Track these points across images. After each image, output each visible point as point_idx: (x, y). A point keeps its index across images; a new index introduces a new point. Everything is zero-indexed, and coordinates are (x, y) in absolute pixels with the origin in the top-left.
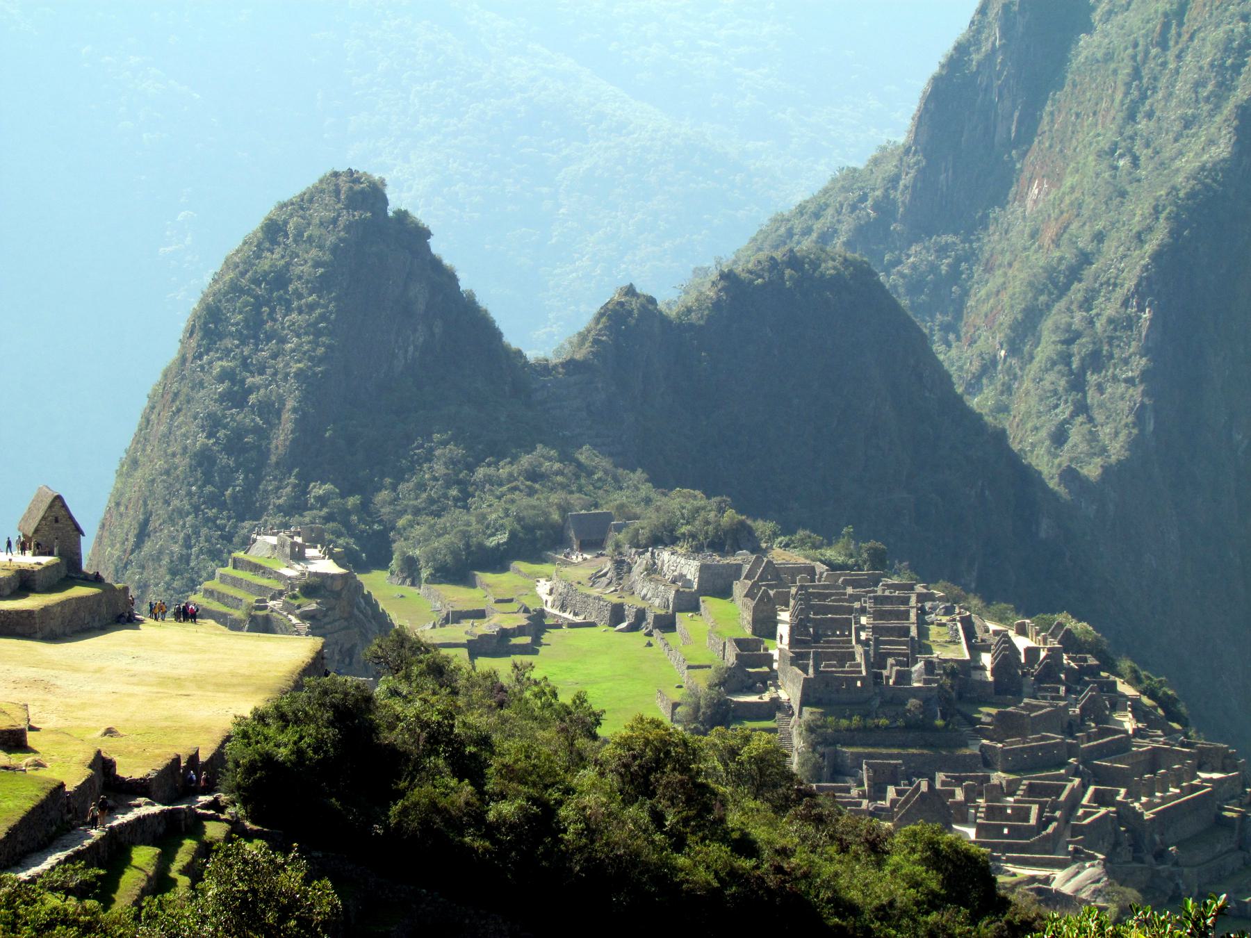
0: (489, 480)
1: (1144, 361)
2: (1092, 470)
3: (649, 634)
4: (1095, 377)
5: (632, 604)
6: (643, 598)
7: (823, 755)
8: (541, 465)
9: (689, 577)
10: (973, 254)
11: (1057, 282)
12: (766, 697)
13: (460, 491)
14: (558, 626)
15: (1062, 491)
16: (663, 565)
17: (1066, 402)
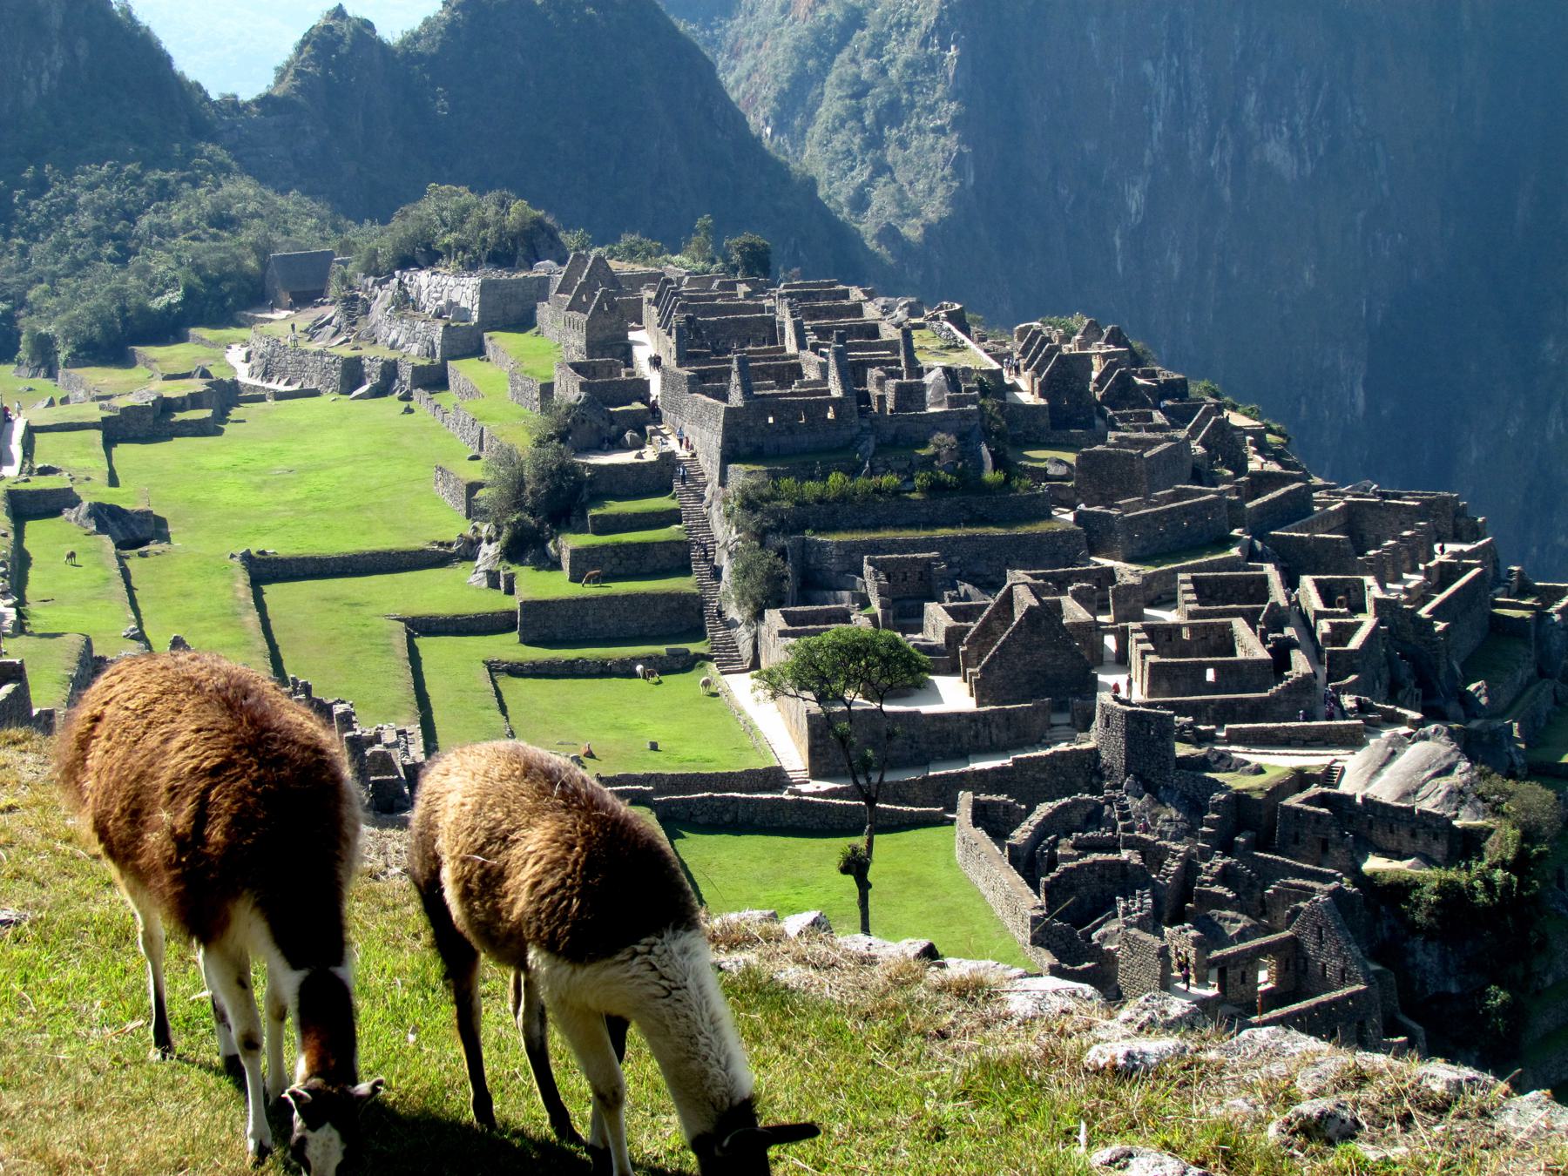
0: (158, 230)
1: (953, 106)
2: (912, 231)
3: (407, 397)
4: (894, 131)
5: (374, 356)
6: (392, 347)
7: (782, 553)
8: (229, 207)
9: (463, 304)
10: (715, 41)
11: (824, 46)
12: (650, 454)
13: (117, 248)
14: (262, 399)
15: (883, 251)
16: (419, 294)
17: (863, 162)
